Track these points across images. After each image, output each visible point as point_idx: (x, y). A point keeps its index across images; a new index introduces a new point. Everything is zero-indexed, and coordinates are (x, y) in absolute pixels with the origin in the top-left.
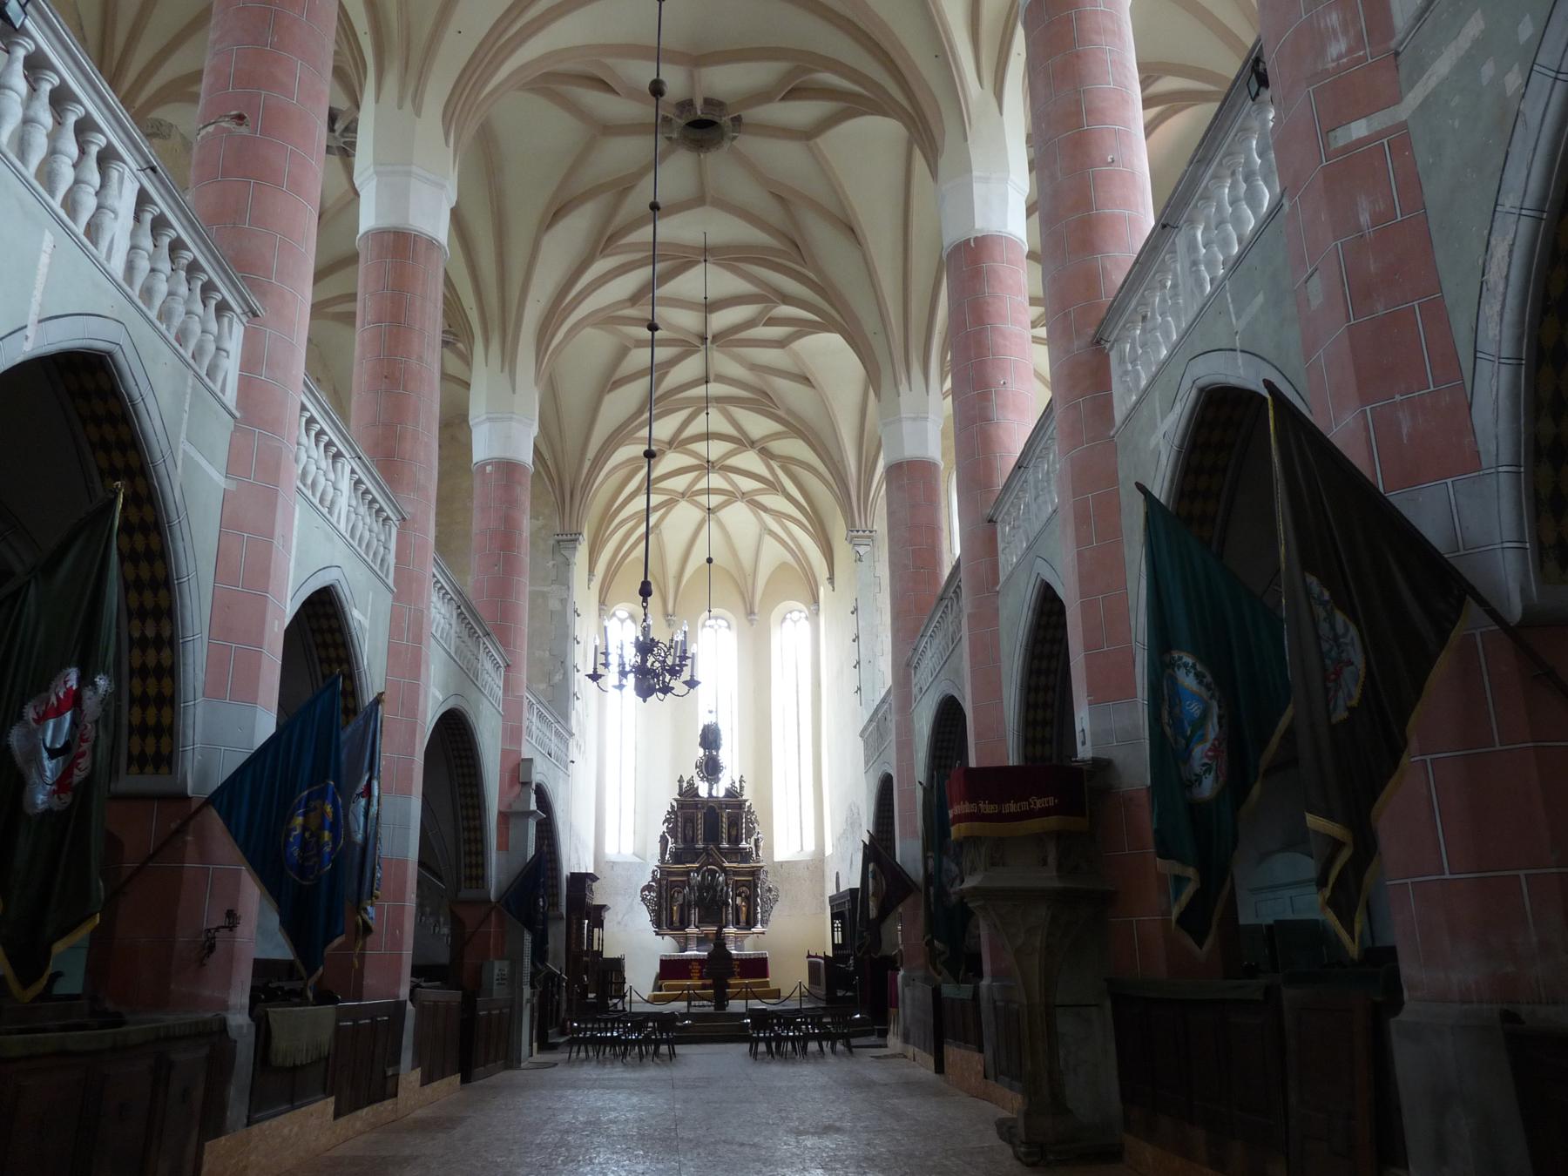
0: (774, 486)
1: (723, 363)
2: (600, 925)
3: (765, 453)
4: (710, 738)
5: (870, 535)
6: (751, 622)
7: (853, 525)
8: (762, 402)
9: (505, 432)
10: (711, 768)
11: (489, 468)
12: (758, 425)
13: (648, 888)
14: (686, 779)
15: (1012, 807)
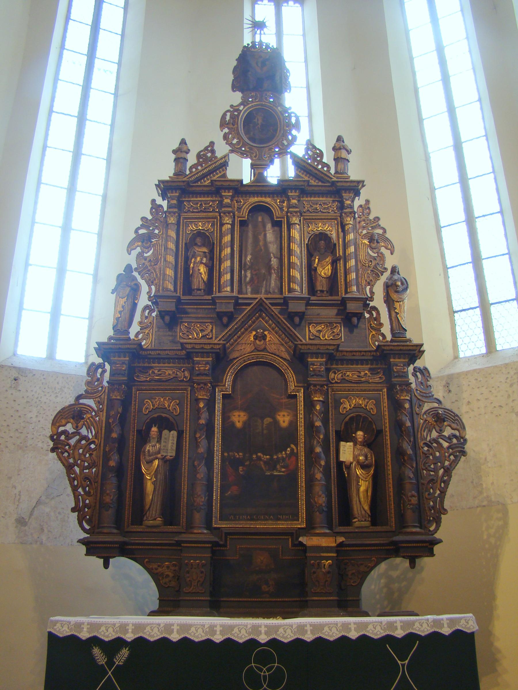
10: (259, 125)
13: (75, 413)
14: (195, 148)
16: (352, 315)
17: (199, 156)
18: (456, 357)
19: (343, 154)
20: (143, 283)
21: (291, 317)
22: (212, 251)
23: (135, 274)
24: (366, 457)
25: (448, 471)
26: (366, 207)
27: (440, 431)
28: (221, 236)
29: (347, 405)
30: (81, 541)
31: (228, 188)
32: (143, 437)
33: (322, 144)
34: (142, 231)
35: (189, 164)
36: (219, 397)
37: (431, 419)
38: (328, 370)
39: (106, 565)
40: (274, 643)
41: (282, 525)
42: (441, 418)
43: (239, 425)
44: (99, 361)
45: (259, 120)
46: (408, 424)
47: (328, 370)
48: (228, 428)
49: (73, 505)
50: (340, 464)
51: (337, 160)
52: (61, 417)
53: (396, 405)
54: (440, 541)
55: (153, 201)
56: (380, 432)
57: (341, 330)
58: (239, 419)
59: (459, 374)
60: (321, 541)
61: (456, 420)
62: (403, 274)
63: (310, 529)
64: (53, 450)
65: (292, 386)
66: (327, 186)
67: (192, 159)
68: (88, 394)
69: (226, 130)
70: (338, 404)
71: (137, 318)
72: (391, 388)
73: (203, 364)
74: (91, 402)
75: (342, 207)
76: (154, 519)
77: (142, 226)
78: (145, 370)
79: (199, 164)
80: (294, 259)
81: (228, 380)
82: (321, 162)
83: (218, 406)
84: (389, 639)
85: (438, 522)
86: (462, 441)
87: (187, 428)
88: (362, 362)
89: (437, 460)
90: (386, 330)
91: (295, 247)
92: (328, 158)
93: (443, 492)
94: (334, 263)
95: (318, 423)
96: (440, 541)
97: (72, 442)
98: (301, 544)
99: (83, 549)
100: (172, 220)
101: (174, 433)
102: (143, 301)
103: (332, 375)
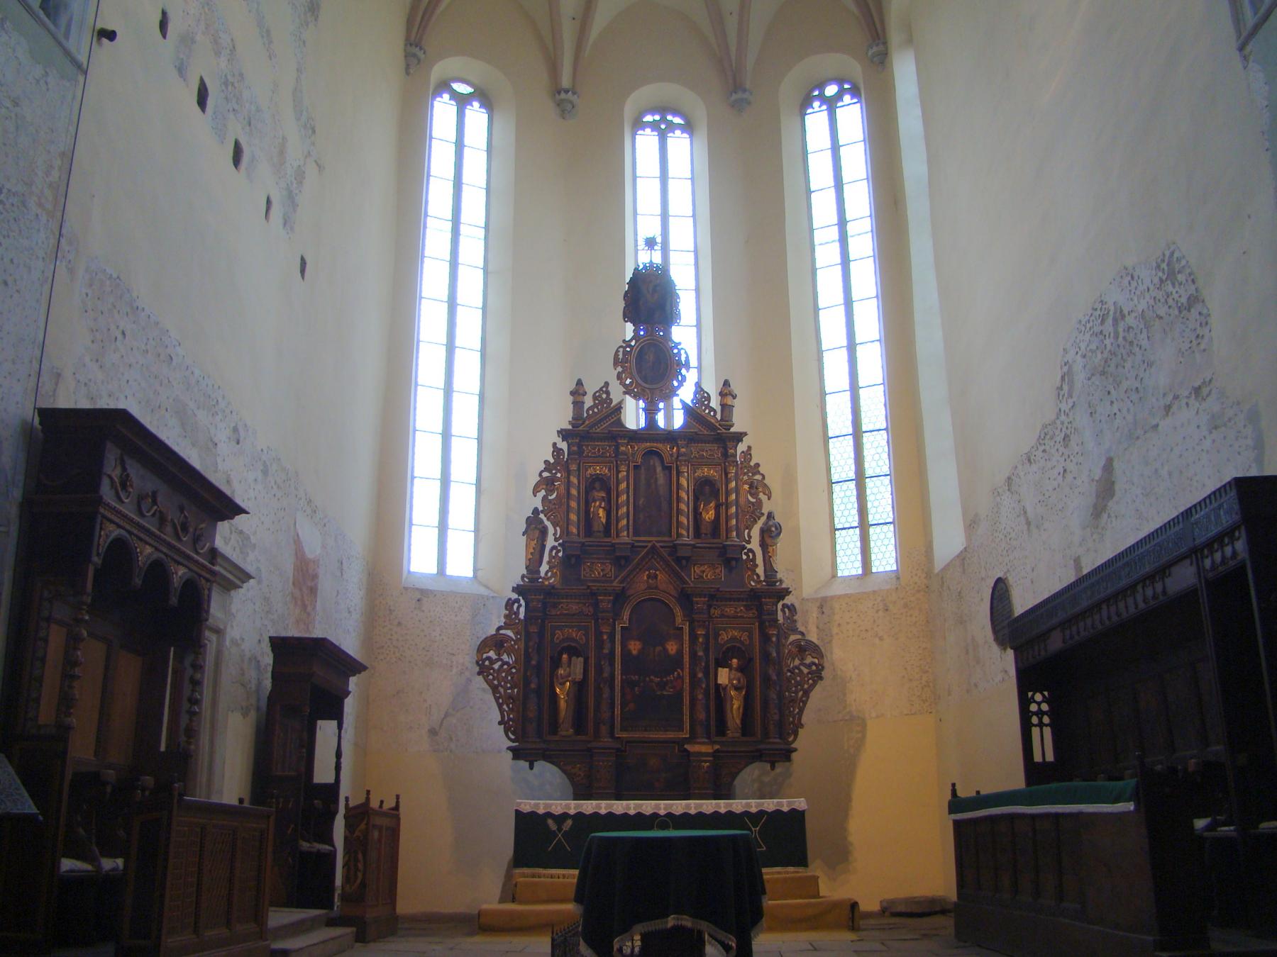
4: (648, 300)
6: (739, 106)
10: (652, 367)
13: (496, 642)
14: (591, 387)
16: (731, 558)
17: (595, 397)
18: (834, 576)
19: (729, 401)
20: (548, 523)
21: (678, 560)
22: (609, 492)
23: (542, 516)
24: (739, 681)
25: (807, 693)
26: (748, 454)
27: (803, 659)
28: (618, 484)
29: (724, 637)
30: (509, 748)
31: (623, 437)
32: (556, 663)
34: (545, 474)
35: (586, 406)
36: (618, 629)
37: (794, 650)
38: (710, 606)
39: (531, 767)
40: (669, 815)
41: (671, 735)
42: (805, 648)
43: (635, 652)
44: (514, 596)
45: (650, 357)
46: (774, 654)
47: (710, 606)
48: (626, 654)
49: (499, 719)
50: (718, 686)
51: (723, 406)
52: (485, 645)
53: (765, 638)
54: (795, 750)
55: (555, 444)
56: (751, 660)
57: (721, 571)
58: (635, 647)
59: (832, 598)
62: (777, 519)
63: (692, 739)
64: (479, 674)
65: (679, 620)
66: (712, 432)
67: (588, 402)
68: (506, 626)
69: (619, 369)
70: (717, 635)
71: (546, 558)
72: (762, 625)
73: (606, 603)
74: (509, 633)
75: (725, 455)
76: (567, 730)
77: (545, 470)
78: (555, 606)
79: (595, 406)
80: (683, 507)
81: (626, 615)
82: (708, 406)
83: (618, 637)
84: (746, 813)
85: (796, 734)
86: (820, 668)
87: (592, 655)
88: (739, 600)
89: (798, 684)
90: (760, 570)
91: (684, 495)
92: (715, 403)
93: (801, 711)
94: (717, 508)
95: (701, 653)
96: (795, 750)
97: (496, 666)
98: (686, 750)
99: (510, 754)
100: (574, 467)
101: (581, 659)
102: (550, 542)
103: (712, 611)
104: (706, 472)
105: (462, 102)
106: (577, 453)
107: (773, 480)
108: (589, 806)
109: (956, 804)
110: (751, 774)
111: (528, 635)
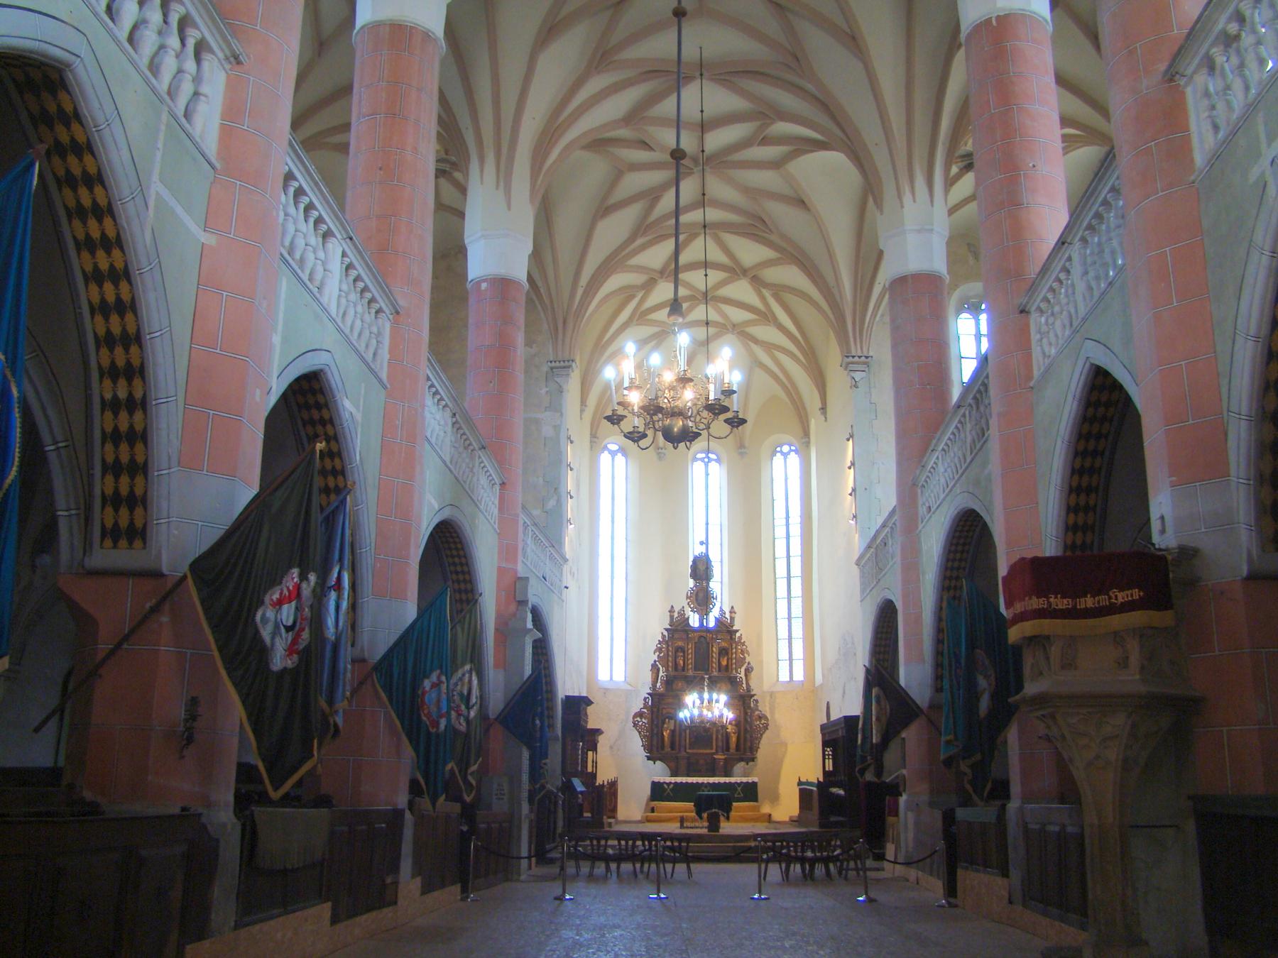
0: (766, 317)
1: (718, 188)
2: (594, 748)
3: (757, 282)
4: (701, 569)
5: (866, 361)
6: (742, 455)
7: (849, 351)
8: (757, 227)
9: (497, 247)
10: (702, 599)
11: (484, 285)
12: (750, 252)
13: (640, 714)
14: (677, 609)
15: (1089, 602)
26: (740, 638)
32: (664, 723)
33: (727, 610)
45: (701, 595)
60: (720, 756)
61: (766, 718)
63: (717, 753)
66: (726, 628)
67: (676, 615)
76: (668, 749)
92: (728, 616)
102: (661, 674)
104: (724, 644)
105: (613, 454)
106: (671, 638)
107: (750, 646)
108: (679, 779)
109: (800, 783)
110: (740, 767)
111: (652, 712)
